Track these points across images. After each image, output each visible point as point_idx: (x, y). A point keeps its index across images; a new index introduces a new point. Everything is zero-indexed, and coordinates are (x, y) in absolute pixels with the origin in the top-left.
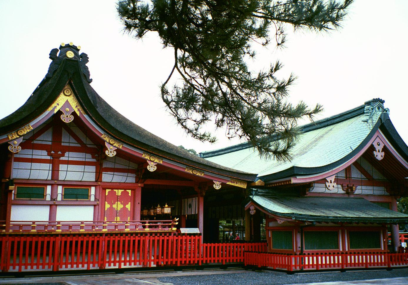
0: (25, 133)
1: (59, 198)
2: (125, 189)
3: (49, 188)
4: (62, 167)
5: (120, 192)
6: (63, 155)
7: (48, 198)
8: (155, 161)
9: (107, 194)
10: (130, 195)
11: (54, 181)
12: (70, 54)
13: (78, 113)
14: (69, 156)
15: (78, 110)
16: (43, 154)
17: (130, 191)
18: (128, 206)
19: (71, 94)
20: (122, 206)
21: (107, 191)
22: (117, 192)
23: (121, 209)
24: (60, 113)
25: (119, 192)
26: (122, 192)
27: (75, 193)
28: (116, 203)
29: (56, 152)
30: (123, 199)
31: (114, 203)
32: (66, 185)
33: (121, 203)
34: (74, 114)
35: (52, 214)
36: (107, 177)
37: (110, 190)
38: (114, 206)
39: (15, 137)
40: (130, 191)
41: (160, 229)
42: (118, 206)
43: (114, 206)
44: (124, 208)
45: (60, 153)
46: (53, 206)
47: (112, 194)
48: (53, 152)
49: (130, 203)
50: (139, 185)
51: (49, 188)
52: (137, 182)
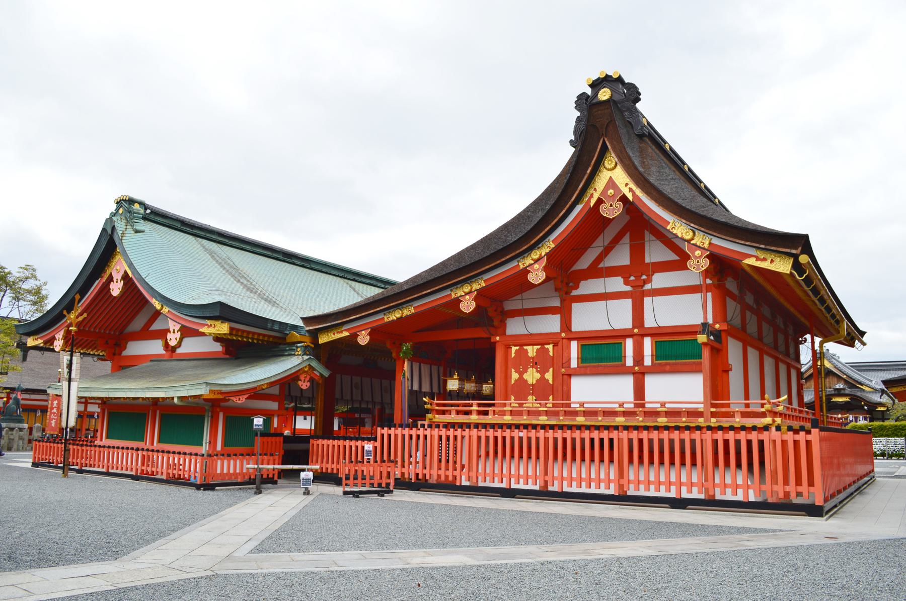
1: (648, 361)
3: (629, 343)
4: (647, 301)
6: (649, 280)
7: (629, 362)
11: (639, 331)
12: (604, 94)
13: (630, 196)
14: (660, 280)
15: (631, 190)
16: (616, 284)
19: (616, 164)
24: (600, 201)
29: (638, 277)
32: (657, 333)
34: (624, 199)
35: (639, 391)
41: (600, 418)
45: (644, 277)
46: (639, 375)
51: (629, 343)
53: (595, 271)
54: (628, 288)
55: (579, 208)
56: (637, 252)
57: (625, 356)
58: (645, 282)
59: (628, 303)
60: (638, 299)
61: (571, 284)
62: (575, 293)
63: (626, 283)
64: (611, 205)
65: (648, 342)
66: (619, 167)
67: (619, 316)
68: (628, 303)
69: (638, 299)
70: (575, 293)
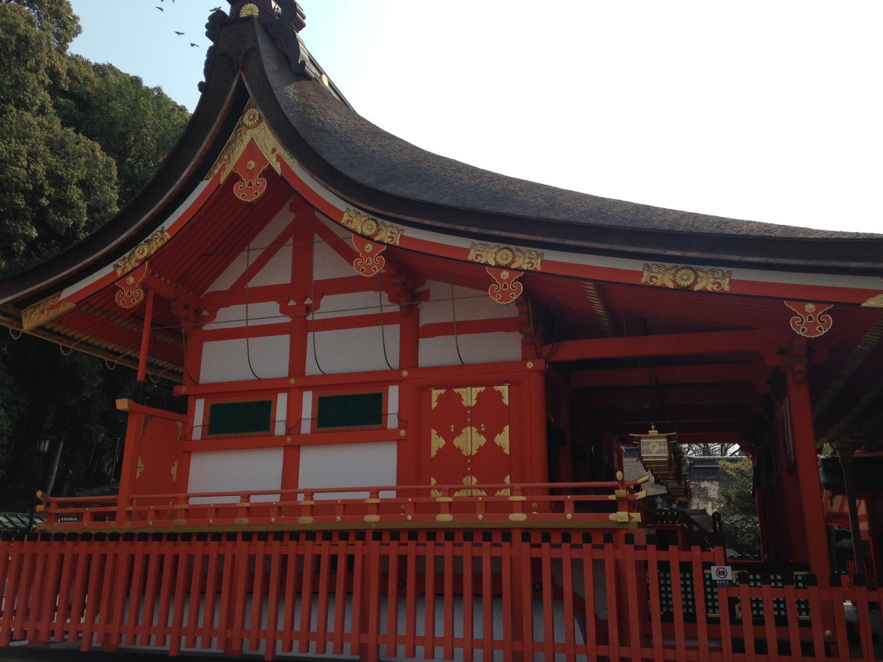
0: (153, 252)
1: (306, 428)
2: (489, 385)
5: (475, 396)
6: (317, 306)
8: (514, 266)
9: (434, 405)
10: (506, 401)
11: (297, 379)
14: (331, 306)
15: (279, 158)
16: (268, 312)
17: (504, 390)
18: (503, 439)
20: (482, 440)
21: (435, 394)
22: (464, 397)
23: (480, 449)
24: (234, 178)
25: (469, 396)
26: (480, 395)
27: (349, 411)
28: (463, 431)
29: (300, 301)
30: (487, 416)
31: (458, 432)
33: (480, 432)
34: (269, 173)
36: (434, 352)
37: (443, 391)
38: (458, 442)
39: (130, 268)
40: (504, 390)
42: (470, 441)
43: (458, 442)
44: (490, 448)
45: (308, 301)
47: (451, 401)
48: (292, 303)
49: (507, 428)
50: (530, 365)
51: (282, 400)
52: (525, 359)
53: (241, 294)
54: (287, 320)
55: (203, 185)
56: (302, 263)
57: (274, 422)
58: (308, 309)
59: (285, 340)
60: (299, 331)
61: (205, 313)
62: (208, 327)
63: (284, 310)
64: (250, 184)
65: (308, 398)
66: (264, 124)
67: (270, 358)
68: (285, 340)
69: (299, 331)
70: (208, 327)
